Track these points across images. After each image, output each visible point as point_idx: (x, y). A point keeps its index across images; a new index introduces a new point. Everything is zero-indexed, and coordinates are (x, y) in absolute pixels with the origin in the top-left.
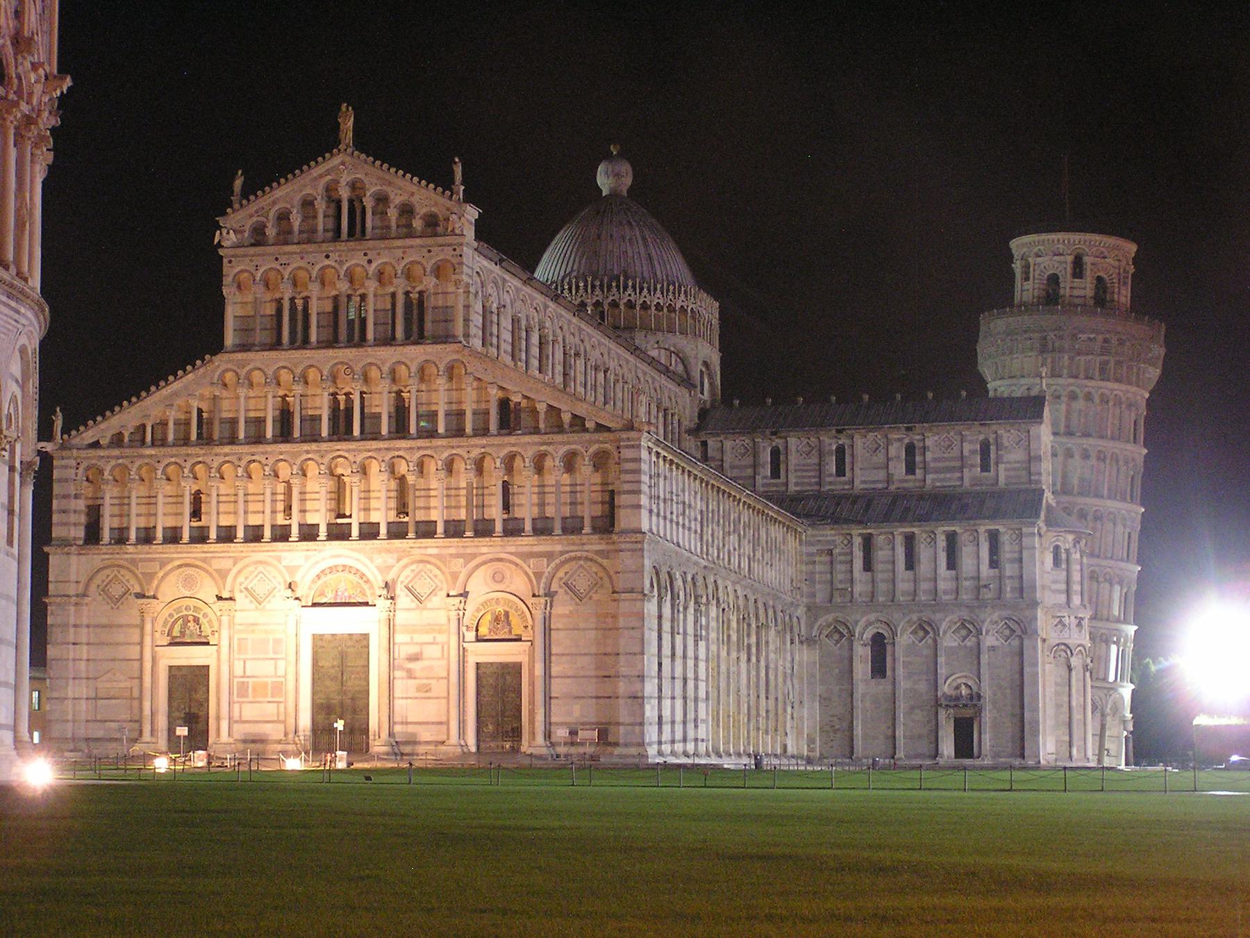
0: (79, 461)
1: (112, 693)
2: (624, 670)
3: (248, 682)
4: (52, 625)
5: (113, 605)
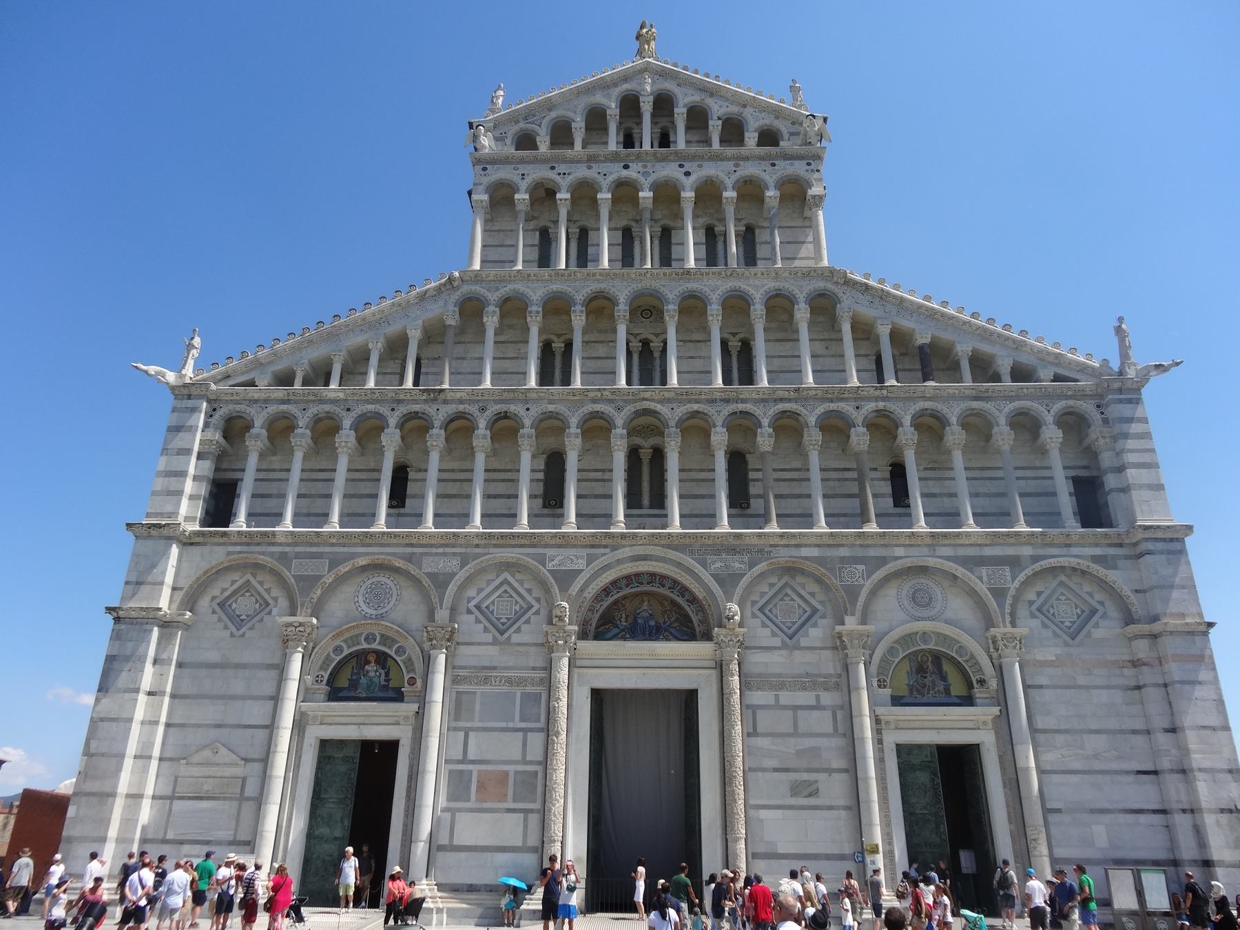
1: (206, 788)
2: (1198, 759)
5: (234, 629)
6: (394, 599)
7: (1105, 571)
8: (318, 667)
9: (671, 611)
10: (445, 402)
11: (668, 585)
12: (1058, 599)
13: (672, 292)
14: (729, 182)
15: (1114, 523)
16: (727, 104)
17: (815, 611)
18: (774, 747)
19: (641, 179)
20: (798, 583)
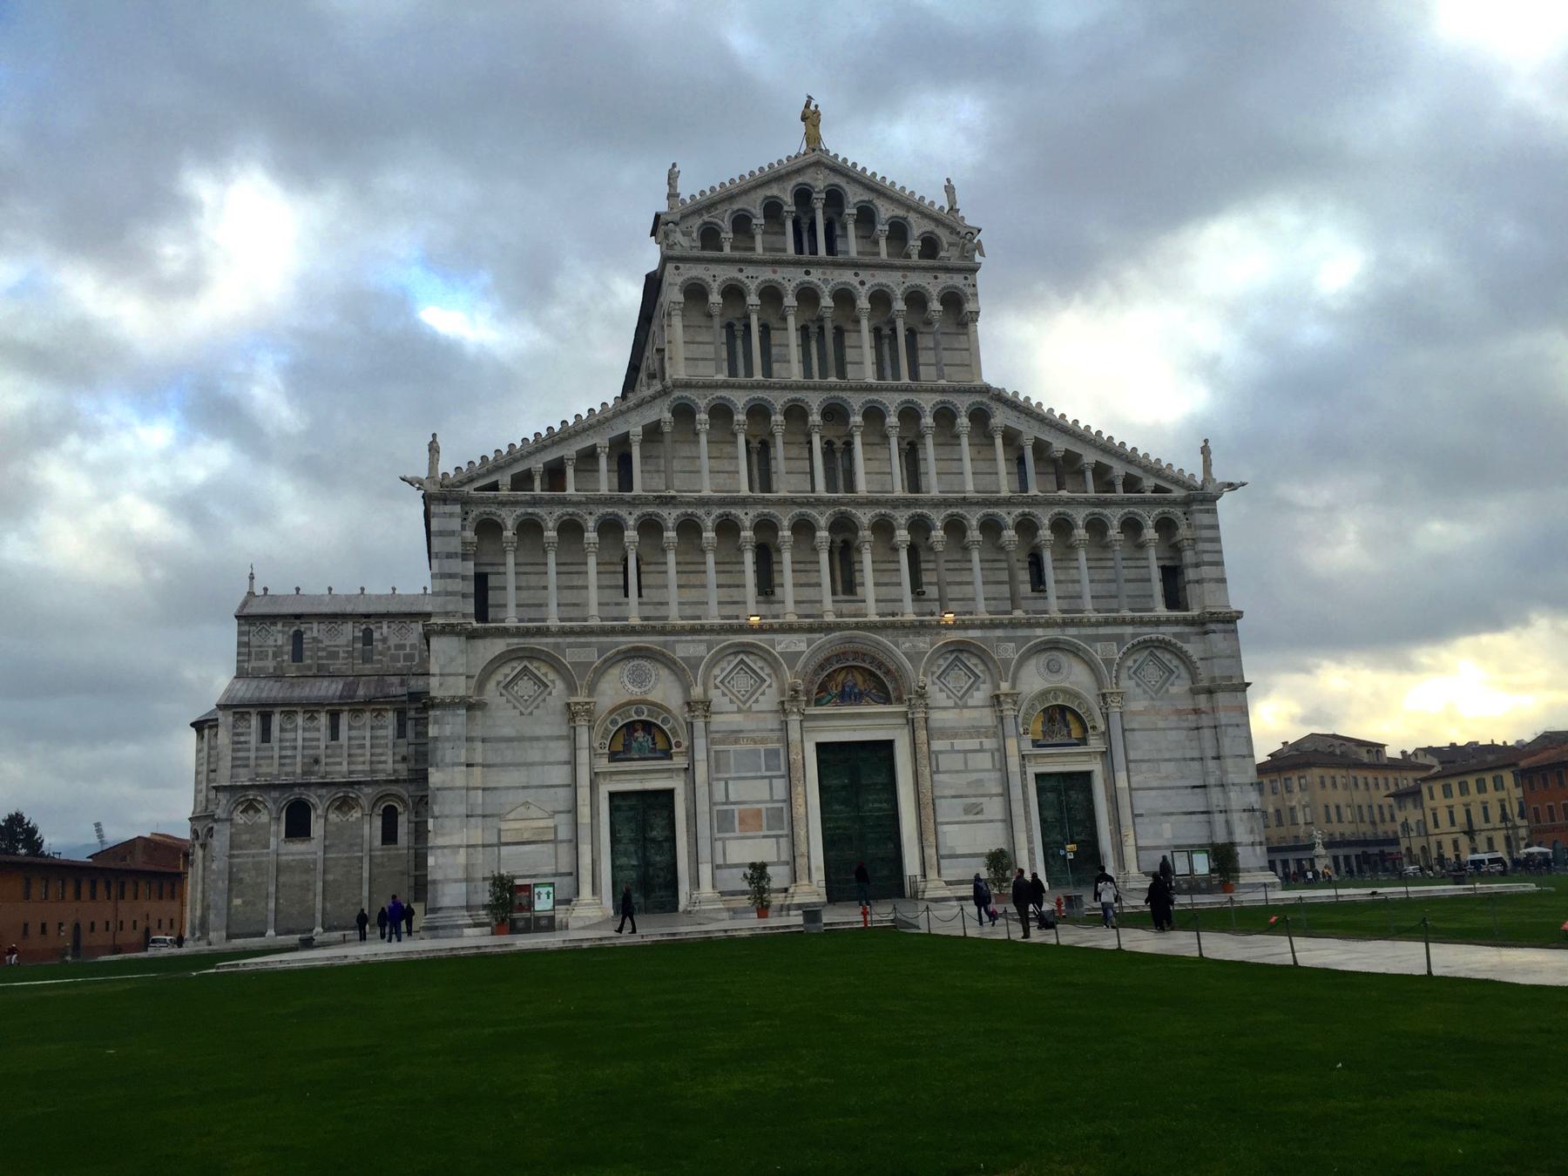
0: (467, 509)
2: (1232, 777)
3: (733, 810)
4: (436, 739)
6: (654, 678)
8: (600, 737)
9: (869, 680)
10: (675, 506)
11: (868, 662)
12: (1147, 664)
13: (856, 402)
14: (899, 292)
15: (1190, 607)
16: (892, 207)
19: (822, 286)
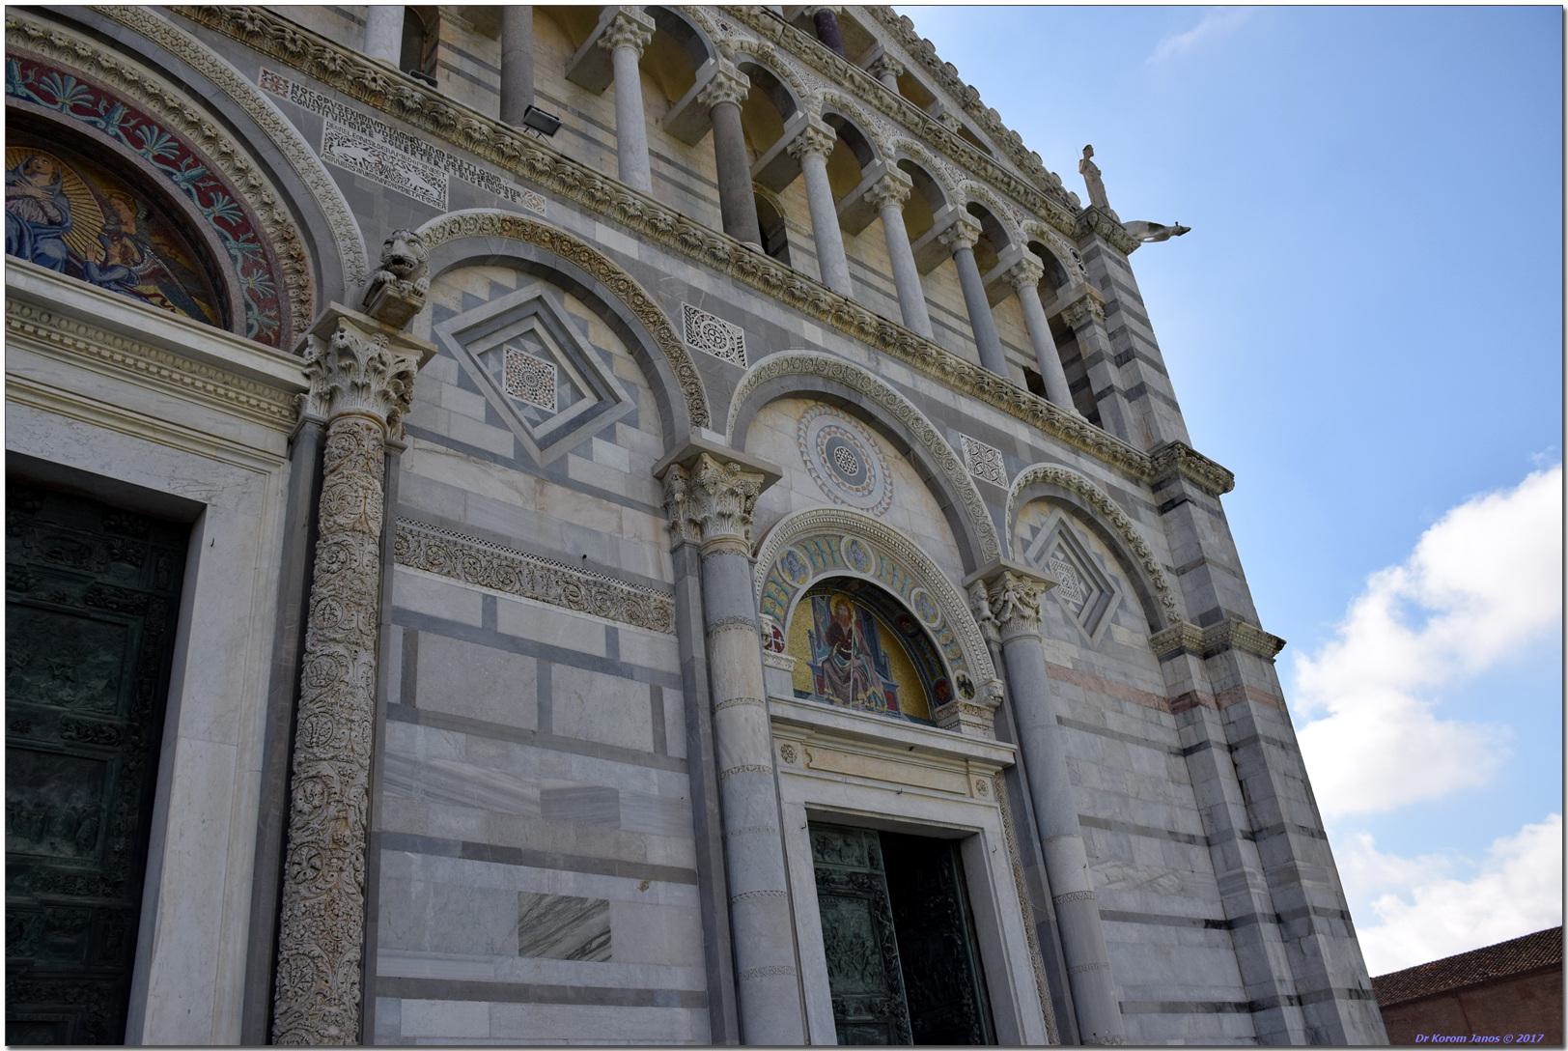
7: (1127, 518)
9: (134, 239)
12: (1053, 555)
17: (606, 396)
18: (468, 770)
20: (573, 316)
